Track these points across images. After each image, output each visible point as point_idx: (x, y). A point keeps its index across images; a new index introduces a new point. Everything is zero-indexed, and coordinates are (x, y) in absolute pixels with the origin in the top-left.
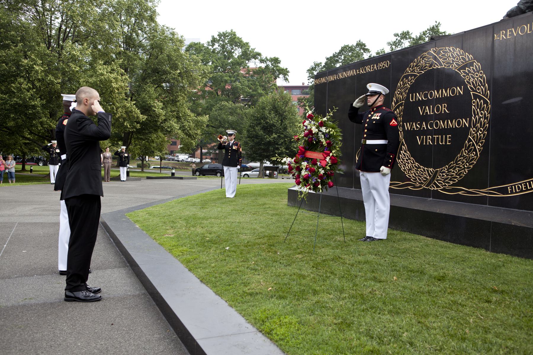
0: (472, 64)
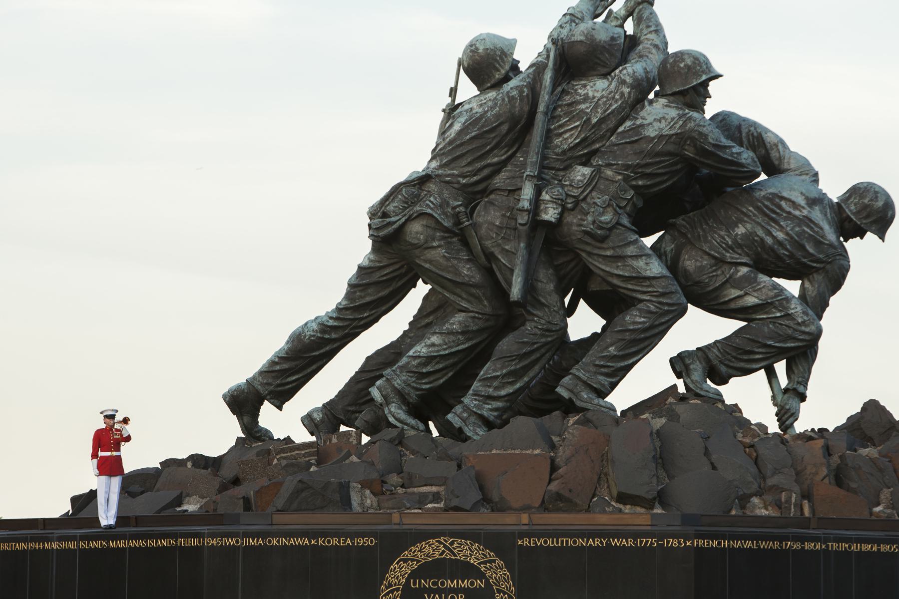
0: (494, 561)
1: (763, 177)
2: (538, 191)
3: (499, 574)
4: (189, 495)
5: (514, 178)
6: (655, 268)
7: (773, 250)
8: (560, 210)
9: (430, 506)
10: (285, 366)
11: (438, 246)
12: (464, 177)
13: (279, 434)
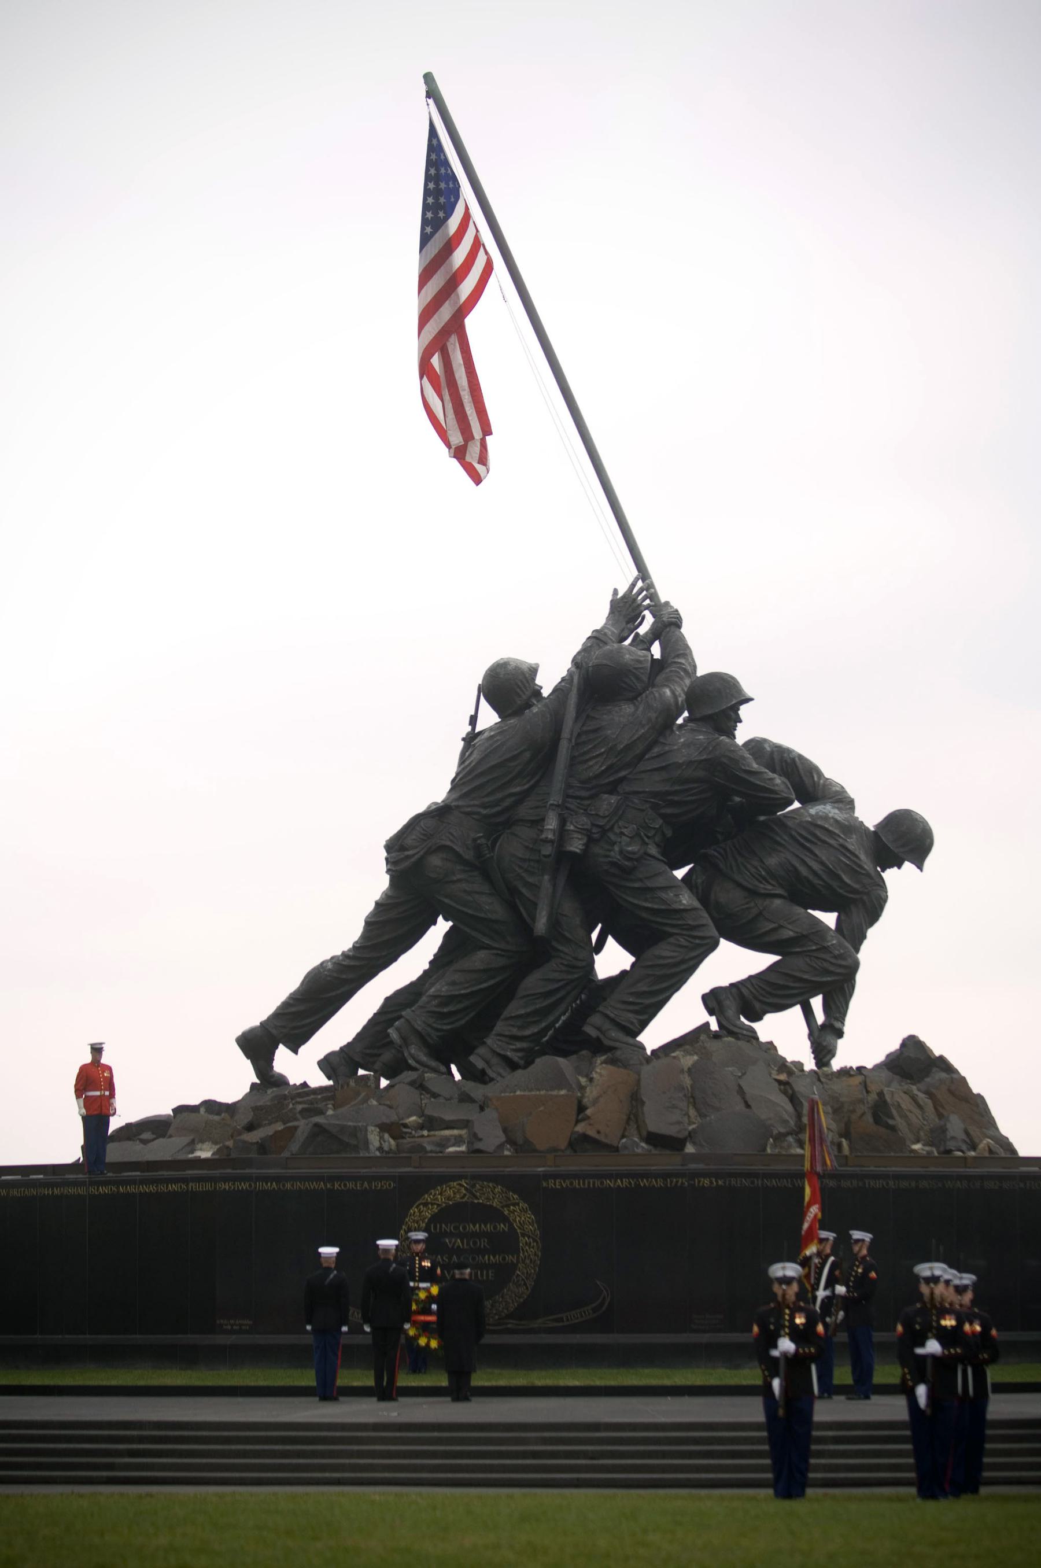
1: (796, 805)
2: (563, 822)
3: (522, 1217)
4: (202, 1141)
5: (537, 807)
6: (686, 899)
7: (808, 881)
8: (585, 841)
9: (451, 1149)
10: (302, 1008)
11: (459, 881)
12: (484, 806)
13: (295, 1079)
